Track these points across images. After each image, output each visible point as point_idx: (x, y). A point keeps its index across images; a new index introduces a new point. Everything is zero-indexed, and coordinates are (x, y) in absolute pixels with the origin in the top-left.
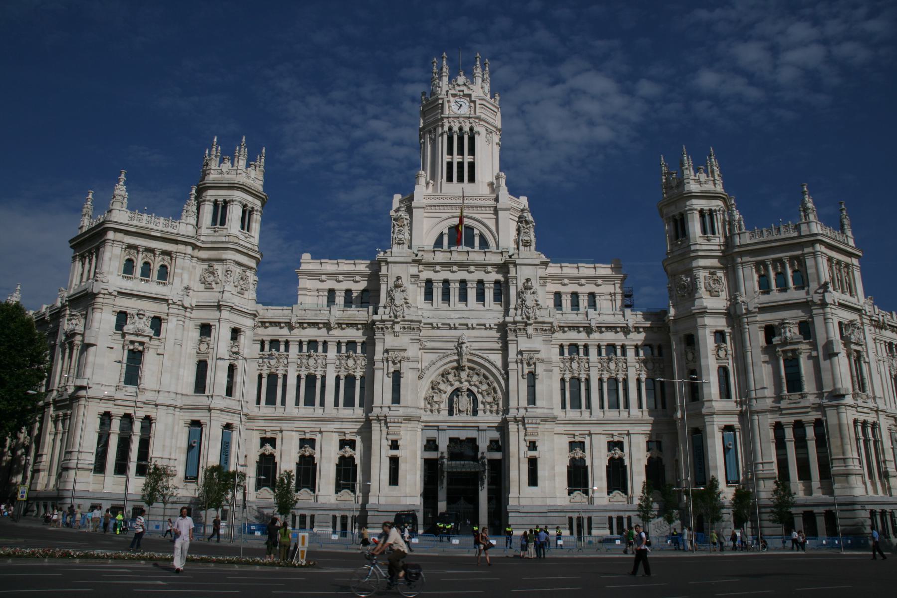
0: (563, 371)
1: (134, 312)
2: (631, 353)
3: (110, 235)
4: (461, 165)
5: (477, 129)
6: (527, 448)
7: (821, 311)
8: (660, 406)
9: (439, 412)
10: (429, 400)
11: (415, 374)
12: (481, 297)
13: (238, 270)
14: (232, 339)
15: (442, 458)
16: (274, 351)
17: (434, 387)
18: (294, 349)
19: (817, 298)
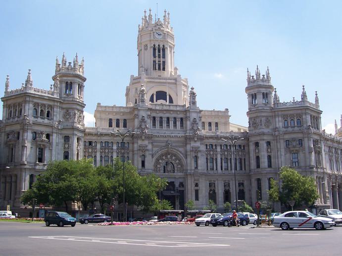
0: (207, 155)
2: (233, 149)
5: (166, 46)
8: (243, 169)
10: (155, 166)
17: (157, 160)
19: (305, 131)
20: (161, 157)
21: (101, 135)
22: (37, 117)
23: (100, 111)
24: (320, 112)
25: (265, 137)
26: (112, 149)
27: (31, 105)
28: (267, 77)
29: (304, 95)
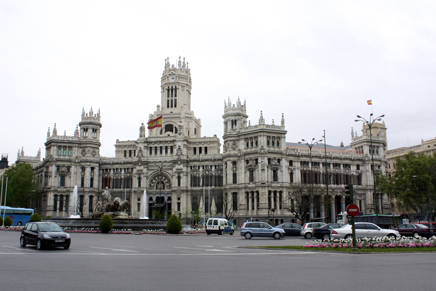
1: (61, 166)
3: (53, 144)
4: (172, 100)
5: (177, 87)
6: (177, 200)
7: (260, 155)
9: (154, 189)
10: (150, 185)
11: (145, 178)
12: (166, 152)
13: (92, 149)
14: (91, 170)
15: (154, 203)
16: (106, 172)
18: (112, 172)
20: (154, 178)
21: (113, 164)
22: (65, 156)
23: (119, 145)
24: (285, 133)
25: (232, 159)
26: (121, 173)
27: (55, 148)
28: (238, 106)
29: (262, 119)
